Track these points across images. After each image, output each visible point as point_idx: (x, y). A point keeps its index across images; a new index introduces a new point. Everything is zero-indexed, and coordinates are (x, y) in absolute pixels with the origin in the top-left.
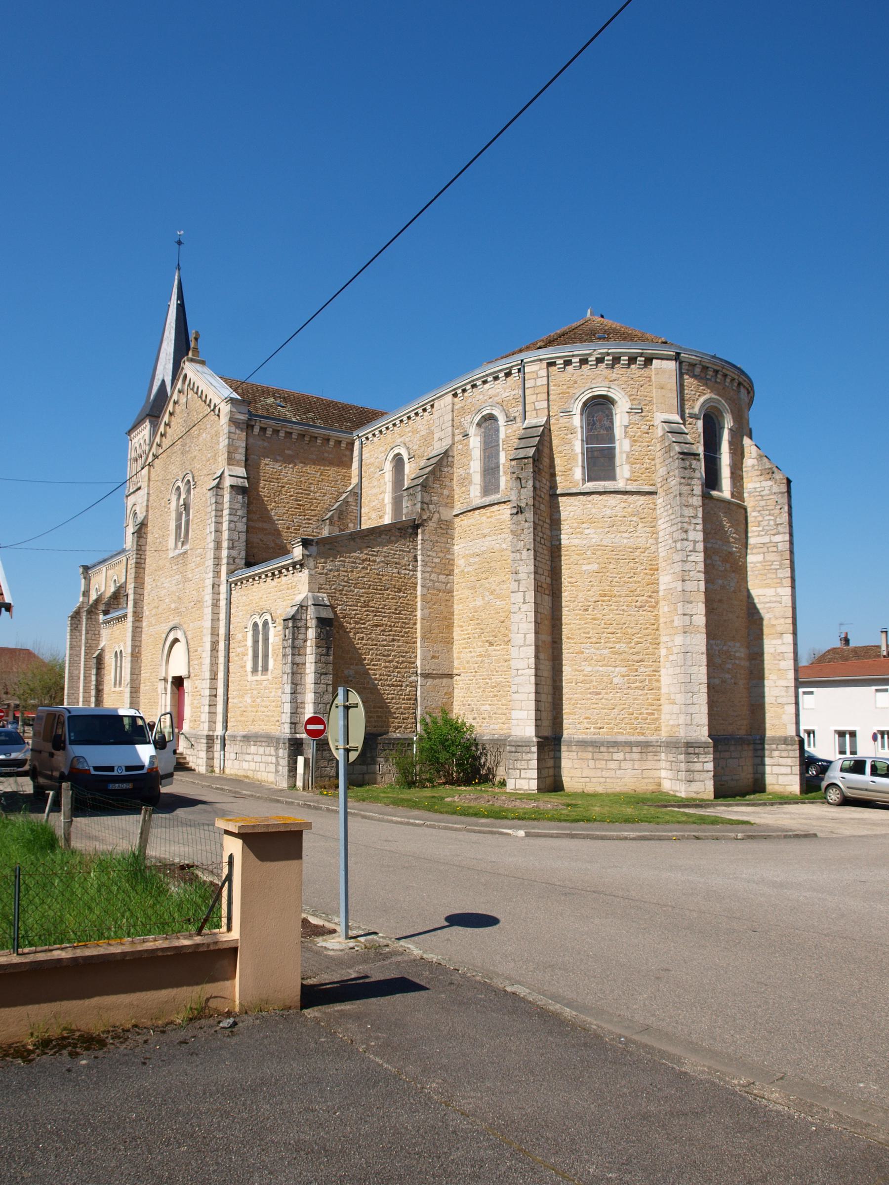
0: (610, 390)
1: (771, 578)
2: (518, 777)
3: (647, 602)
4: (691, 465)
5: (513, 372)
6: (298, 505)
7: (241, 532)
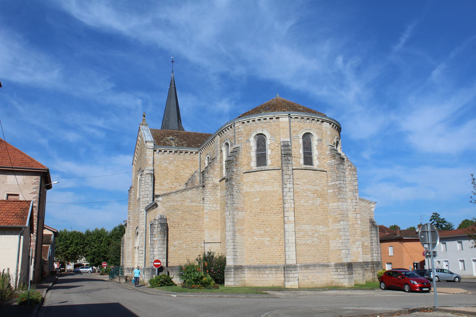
0: (263, 131)
1: (335, 199)
2: (228, 281)
3: (278, 212)
4: (288, 159)
5: (232, 126)
6: (175, 178)
7: (151, 191)
